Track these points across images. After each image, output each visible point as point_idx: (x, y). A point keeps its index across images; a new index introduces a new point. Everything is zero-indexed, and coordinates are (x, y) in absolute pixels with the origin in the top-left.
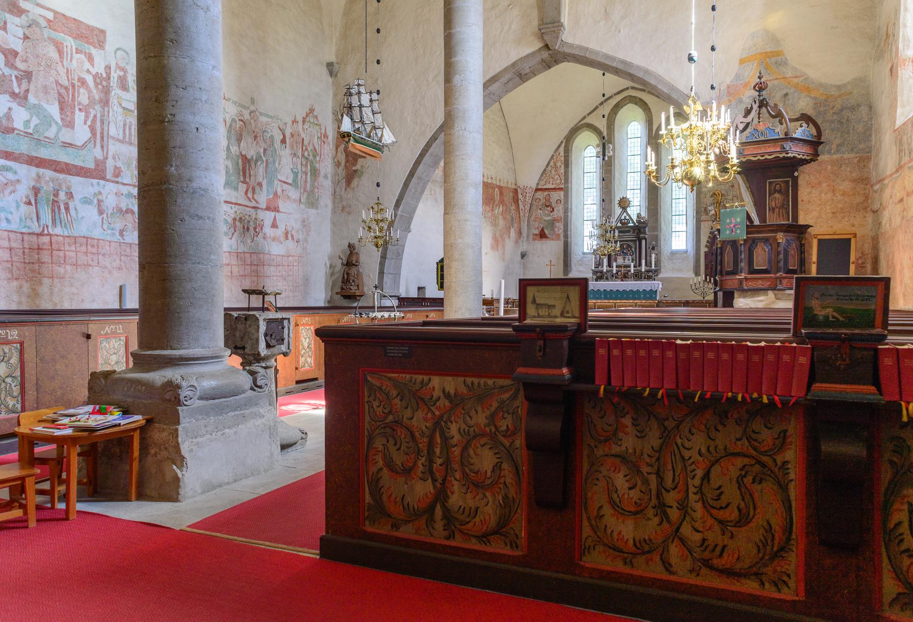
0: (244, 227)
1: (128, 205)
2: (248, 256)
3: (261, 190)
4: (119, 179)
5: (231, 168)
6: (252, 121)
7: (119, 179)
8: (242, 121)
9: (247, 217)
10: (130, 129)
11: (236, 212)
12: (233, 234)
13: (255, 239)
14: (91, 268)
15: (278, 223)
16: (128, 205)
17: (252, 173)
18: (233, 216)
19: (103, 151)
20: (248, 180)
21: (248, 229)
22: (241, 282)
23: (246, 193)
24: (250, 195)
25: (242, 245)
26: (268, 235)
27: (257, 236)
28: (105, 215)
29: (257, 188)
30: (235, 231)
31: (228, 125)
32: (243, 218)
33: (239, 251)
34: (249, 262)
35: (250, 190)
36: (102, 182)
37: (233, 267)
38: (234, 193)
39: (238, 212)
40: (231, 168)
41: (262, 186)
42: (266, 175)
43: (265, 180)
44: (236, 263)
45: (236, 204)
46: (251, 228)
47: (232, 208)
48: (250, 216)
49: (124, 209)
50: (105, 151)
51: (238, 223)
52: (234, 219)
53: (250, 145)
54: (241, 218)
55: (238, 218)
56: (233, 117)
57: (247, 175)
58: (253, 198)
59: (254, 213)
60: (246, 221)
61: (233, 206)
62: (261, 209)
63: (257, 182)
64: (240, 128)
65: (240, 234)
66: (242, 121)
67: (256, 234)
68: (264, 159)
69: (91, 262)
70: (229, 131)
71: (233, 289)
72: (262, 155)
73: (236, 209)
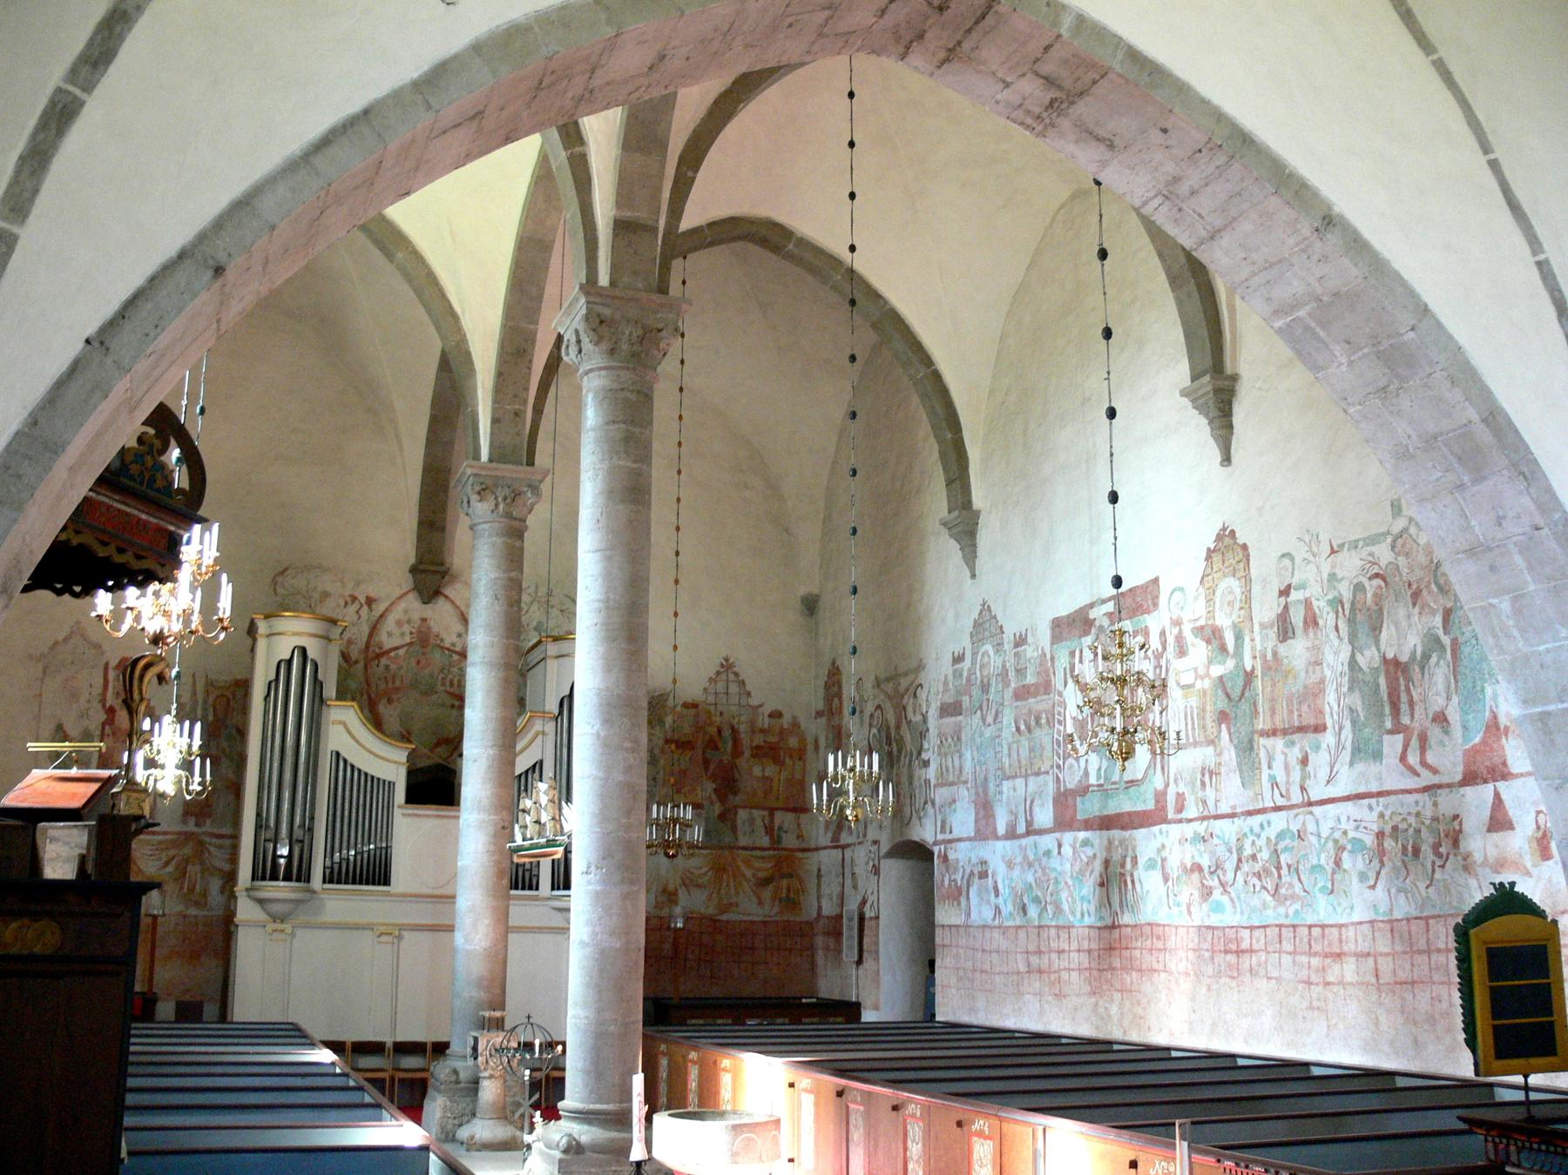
0: (1404, 848)
1: (1193, 856)
2: (1417, 927)
3: (1447, 732)
4: (1184, 815)
5: (1360, 709)
6: (1402, 561)
7: (1184, 815)
8: (1377, 575)
9: (1412, 820)
10: (1192, 719)
11: (1381, 815)
12: (1378, 873)
13: (1438, 875)
14: (1156, 974)
15: (1512, 812)
16: (1193, 856)
17: (1415, 698)
18: (1375, 827)
19: (1164, 774)
20: (1405, 720)
21: (1416, 852)
22: (1403, 999)
23: (1403, 758)
24: (1413, 759)
25: (1402, 897)
26: (1478, 857)
27: (1443, 866)
28: (1170, 883)
29: (1435, 733)
30: (1382, 863)
31: (1347, 606)
32: (1402, 826)
33: (1397, 915)
34: (1422, 944)
35: (1415, 743)
36: (1164, 827)
37: (1380, 959)
38: (1374, 768)
39: (1388, 813)
40: (1360, 709)
41: (1446, 720)
42: (1456, 682)
43: (1455, 699)
44: (1387, 950)
45: (1380, 794)
46: (1426, 849)
47: (1371, 808)
48: (1418, 814)
49: (1189, 866)
50: (1166, 769)
51: (1389, 843)
52: (1380, 835)
53: (1404, 623)
54: (1395, 828)
55: (1388, 829)
56: (1355, 581)
57: (1404, 707)
58: (1424, 763)
59: (1429, 804)
60: (1411, 831)
61: (1373, 801)
62: (1449, 786)
63: (1431, 716)
64: (1375, 595)
65: (1395, 869)
66: (1377, 575)
67: (1439, 863)
68: (1446, 640)
69: (1155, 966)
70: (1351, 622)
71: (1382, 1019)
72: (1440, 632)
73: (1380, 808)
